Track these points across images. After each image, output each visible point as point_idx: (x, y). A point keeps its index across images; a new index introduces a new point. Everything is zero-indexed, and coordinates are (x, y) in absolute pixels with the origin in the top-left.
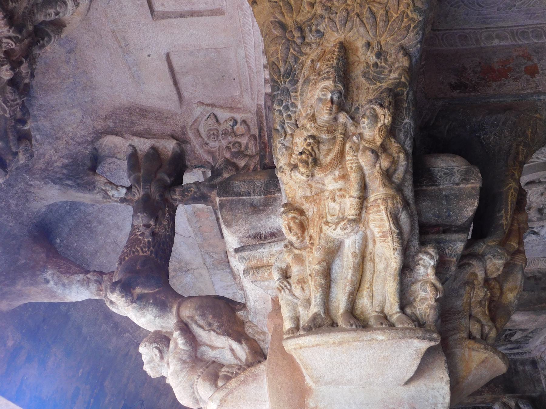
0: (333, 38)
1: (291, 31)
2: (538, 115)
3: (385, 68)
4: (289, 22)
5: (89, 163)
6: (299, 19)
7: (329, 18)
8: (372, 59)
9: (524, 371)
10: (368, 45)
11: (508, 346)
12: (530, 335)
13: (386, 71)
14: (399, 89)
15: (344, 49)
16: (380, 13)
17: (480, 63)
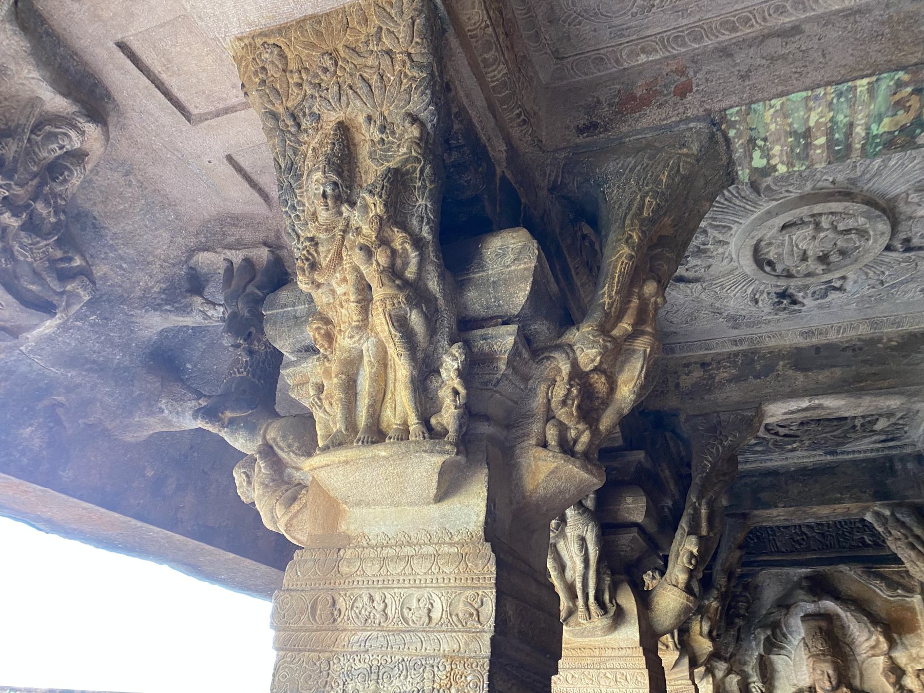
0: (331, 118)
1: (284, 120)
2: (685, 150)
3: (393, 143)
4: (281, 110)
5: (186, 285)
6: (289, 105)
7: (321, 96)
8: (377, 136)
9: (905, 469)
10: (369, 118)
11: (875, 438)
12: (901, 422)
13: (395, 148)
14: (409, 166)
15: (343, 129)
16: (374, 80)
17: (619, 92)
